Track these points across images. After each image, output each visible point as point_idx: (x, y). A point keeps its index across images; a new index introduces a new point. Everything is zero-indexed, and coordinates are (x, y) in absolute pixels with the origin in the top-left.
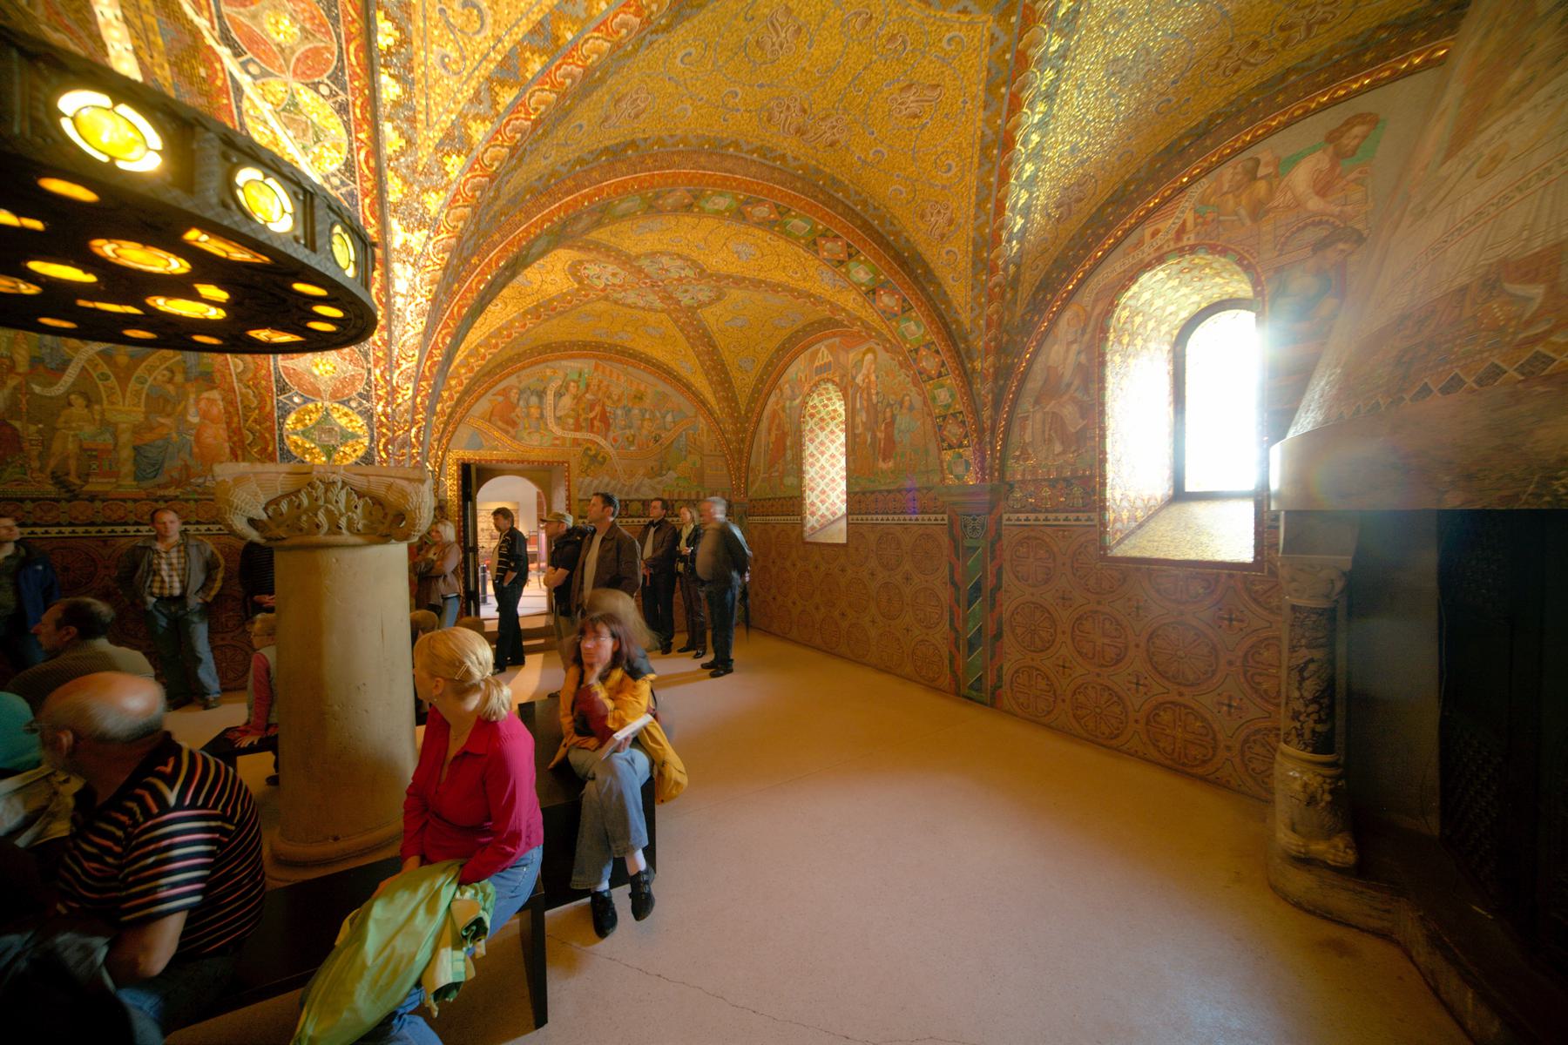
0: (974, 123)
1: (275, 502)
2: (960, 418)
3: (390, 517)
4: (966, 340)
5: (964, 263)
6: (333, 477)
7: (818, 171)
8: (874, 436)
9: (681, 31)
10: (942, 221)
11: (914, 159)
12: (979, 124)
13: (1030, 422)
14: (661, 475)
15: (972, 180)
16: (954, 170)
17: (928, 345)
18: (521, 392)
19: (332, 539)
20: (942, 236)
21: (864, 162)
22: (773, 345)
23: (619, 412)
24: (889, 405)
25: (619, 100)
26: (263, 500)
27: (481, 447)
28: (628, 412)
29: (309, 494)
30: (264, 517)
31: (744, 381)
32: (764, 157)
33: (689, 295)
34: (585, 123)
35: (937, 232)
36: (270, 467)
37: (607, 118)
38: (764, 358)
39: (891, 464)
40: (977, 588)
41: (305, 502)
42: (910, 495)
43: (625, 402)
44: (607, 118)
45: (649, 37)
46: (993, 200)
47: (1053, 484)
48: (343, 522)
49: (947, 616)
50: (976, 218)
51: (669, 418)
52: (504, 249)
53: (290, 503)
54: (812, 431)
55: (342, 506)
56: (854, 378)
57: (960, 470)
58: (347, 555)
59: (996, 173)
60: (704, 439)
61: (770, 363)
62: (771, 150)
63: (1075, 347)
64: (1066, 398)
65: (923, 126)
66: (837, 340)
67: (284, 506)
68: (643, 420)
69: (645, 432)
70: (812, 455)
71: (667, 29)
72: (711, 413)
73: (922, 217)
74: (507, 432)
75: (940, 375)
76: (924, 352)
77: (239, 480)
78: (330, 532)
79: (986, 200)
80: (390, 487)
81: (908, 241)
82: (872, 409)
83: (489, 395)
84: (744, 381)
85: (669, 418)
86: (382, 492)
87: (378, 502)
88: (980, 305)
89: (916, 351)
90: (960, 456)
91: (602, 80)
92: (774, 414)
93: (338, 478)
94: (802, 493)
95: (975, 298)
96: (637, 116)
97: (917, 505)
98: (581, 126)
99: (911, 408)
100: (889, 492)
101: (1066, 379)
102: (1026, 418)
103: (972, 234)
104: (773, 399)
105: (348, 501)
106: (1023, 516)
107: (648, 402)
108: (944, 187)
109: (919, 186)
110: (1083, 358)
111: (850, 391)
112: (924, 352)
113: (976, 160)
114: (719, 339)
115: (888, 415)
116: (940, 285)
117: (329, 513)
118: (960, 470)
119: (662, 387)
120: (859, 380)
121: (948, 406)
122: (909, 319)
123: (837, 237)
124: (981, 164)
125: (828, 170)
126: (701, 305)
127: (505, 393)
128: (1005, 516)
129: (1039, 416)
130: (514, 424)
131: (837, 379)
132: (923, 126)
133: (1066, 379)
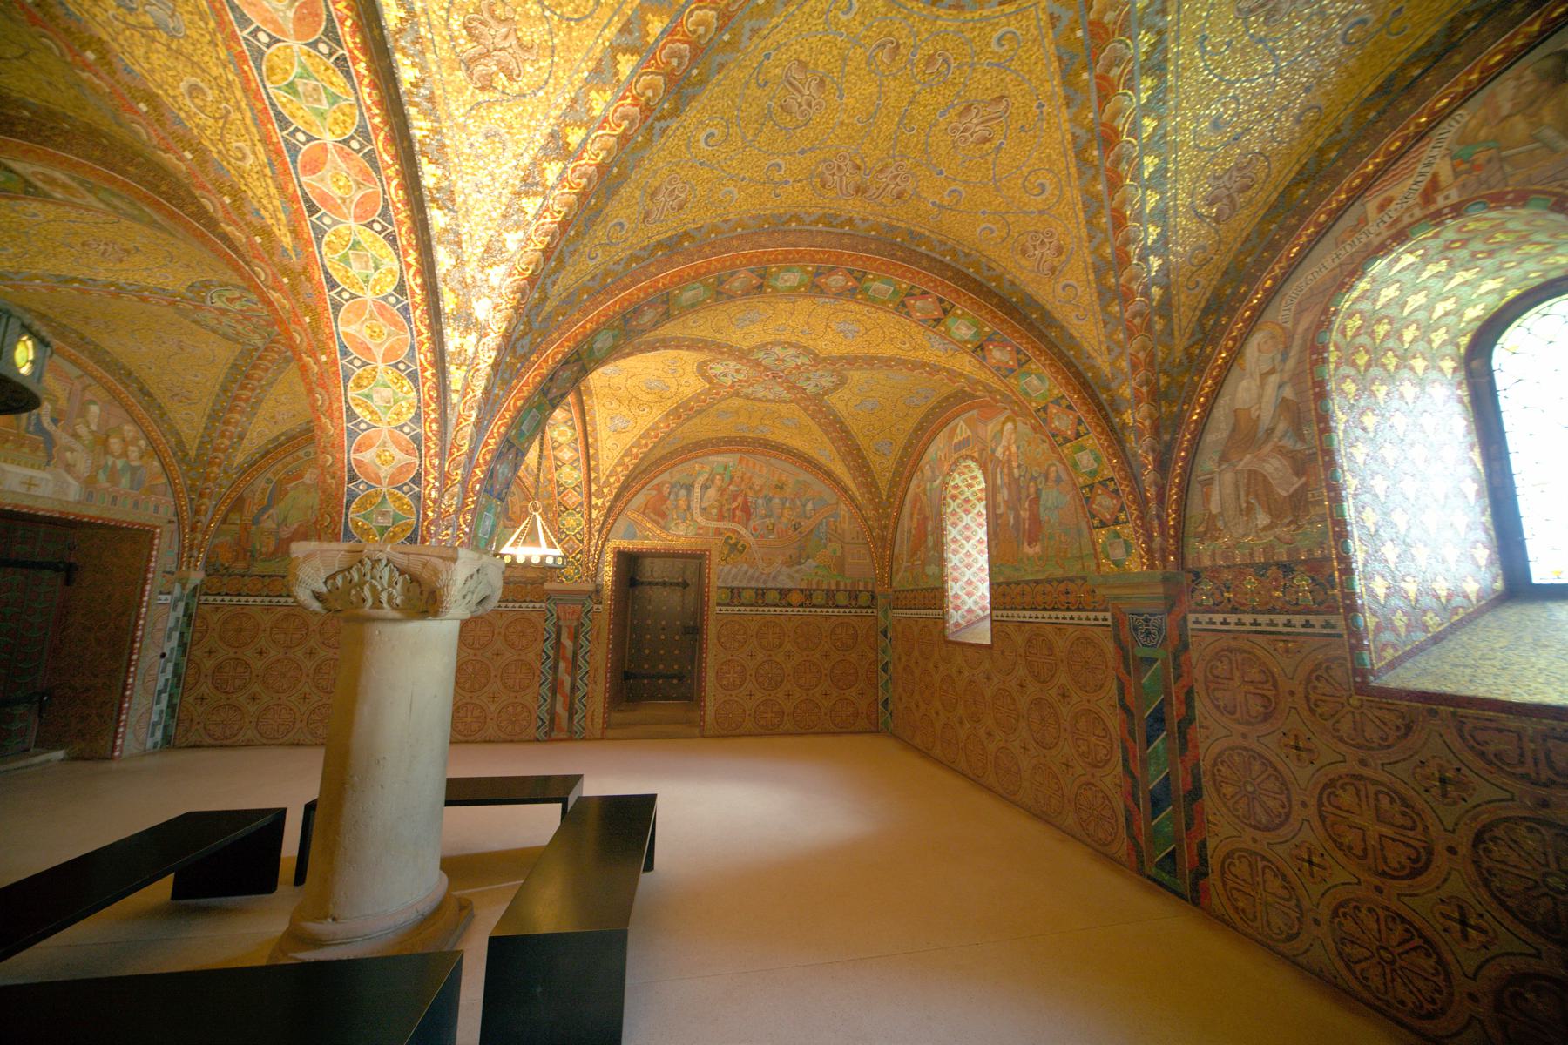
0: (1059, 127)
1: (332, 577)
2: (1112, 486)
3: (426, 594)
4: (1108, 390)
5: (1087, 295)
6: (379, 555)
7: (892, 228)
8: (1017, 516)
9: (692, 113)
10: (1048, 252)
11: (998, 189)
12: (1066, 126)
13: (1216, 487)
14: (799, 563)
15: (1074, 194)
16: (1049, 189)
17: (1057, 402)
18: (672, 486)
19: (375, 612)
20: (1053, 270)
21: (941, 207)
22: (911, 424)
23: (760, 502)
24: (1033, 478)
25: (653, 195)
26: (324, 575)
27: (634, 536)
28: (769, 500)
29: (359, 570)
30: (324, 590)
31: (883, 465)
32: (830, 224)
33: (812, 383)
34: (624, 220)
35: (1046, 267)
36: (334, 546)
37: (648, 214)
38: (902, 439)
39: (1038, 549)
40: (1158, 718)
41: (356, 578)
42: (1062, 587)
43: (766, 492)
44: (648, 214)
45: (657, 125)
46: (1106, 211)
47: (1261, 570)
48: (384, 597)
49: (1119, 753)
50: (1091, 238)
51: (810, 506)
52: (561, 345)
53: (345, 578)
54: (954, 513)
55: (385, 581)
56: (993, 452)
57: (1119, 553)
58: (388, 629)
59: (1102, 179)
60: (846, 526)
61: (909, 445)
62: (836, 217)
63: (1274, 379)
64: (1268, 448)
65: (998, 149)
66: (975, 412)
67: (339, 581)
68: (783, 508)
69: (785, 520)
70: (955, 541)
71: (675, 112)
72: (852, 499)
73: (1024, 252)
74: (658, 523)
75: (1078, 435)
76: (1053, 410)
77: (308, 557)
78: (373, 606)
79: (1097, 213)
80: (425, 565)
81: (1012, 283)
82: (1014, 484)
83: (645, 491)
84: (883, 465)
85: (810, 506)
86: (418, 570)
87: (415, 579)
88: (1118, 343)
89: (1045, 409)
90: (1118, 536)
91: (623, 177)
92: (917, 498)
93: (383, 556)
94: (944, 582)
95: (1109, 336)
96: (681, 207)
97: (1072, 598)
98: (621, 224)
99: (1058, 480)
100: (1037, 582)
101: (1266, 421)
102: (1209, 483)
103: (1090, 260)
104: (914, 482)
105: (391, 577)
106: (1218, 618)
107: (788, 491)
108: (1041, 212)
109: (1011, 218)
110: (1288, 392)
111: (990, 466)
112: (1053, 410)
113: (1073, 170)
114: (854, 427)
115: (1032, 490)
116: (1062, 327)
117: (373, 589)
118: (1119, 553)
119: (804, 476)
120: (999, 452)
121: (1093, 473)
122: (1028, 374)
123: (925, 293)
124: (1081, 173)
125: (903, 225)
126: (827, 391)
127: (658, 488)
128: (1191, 617)
129: (1228, 477)
130: (663, 515)
131: (976, 455)
132: (998, 149)
133: (1266, 421)
